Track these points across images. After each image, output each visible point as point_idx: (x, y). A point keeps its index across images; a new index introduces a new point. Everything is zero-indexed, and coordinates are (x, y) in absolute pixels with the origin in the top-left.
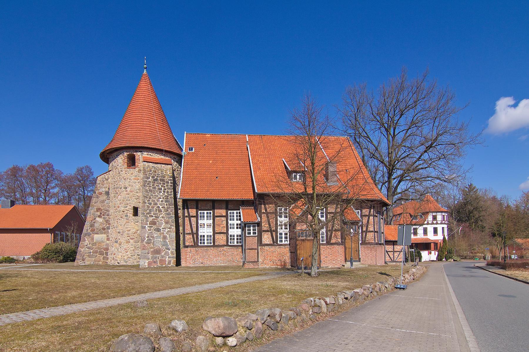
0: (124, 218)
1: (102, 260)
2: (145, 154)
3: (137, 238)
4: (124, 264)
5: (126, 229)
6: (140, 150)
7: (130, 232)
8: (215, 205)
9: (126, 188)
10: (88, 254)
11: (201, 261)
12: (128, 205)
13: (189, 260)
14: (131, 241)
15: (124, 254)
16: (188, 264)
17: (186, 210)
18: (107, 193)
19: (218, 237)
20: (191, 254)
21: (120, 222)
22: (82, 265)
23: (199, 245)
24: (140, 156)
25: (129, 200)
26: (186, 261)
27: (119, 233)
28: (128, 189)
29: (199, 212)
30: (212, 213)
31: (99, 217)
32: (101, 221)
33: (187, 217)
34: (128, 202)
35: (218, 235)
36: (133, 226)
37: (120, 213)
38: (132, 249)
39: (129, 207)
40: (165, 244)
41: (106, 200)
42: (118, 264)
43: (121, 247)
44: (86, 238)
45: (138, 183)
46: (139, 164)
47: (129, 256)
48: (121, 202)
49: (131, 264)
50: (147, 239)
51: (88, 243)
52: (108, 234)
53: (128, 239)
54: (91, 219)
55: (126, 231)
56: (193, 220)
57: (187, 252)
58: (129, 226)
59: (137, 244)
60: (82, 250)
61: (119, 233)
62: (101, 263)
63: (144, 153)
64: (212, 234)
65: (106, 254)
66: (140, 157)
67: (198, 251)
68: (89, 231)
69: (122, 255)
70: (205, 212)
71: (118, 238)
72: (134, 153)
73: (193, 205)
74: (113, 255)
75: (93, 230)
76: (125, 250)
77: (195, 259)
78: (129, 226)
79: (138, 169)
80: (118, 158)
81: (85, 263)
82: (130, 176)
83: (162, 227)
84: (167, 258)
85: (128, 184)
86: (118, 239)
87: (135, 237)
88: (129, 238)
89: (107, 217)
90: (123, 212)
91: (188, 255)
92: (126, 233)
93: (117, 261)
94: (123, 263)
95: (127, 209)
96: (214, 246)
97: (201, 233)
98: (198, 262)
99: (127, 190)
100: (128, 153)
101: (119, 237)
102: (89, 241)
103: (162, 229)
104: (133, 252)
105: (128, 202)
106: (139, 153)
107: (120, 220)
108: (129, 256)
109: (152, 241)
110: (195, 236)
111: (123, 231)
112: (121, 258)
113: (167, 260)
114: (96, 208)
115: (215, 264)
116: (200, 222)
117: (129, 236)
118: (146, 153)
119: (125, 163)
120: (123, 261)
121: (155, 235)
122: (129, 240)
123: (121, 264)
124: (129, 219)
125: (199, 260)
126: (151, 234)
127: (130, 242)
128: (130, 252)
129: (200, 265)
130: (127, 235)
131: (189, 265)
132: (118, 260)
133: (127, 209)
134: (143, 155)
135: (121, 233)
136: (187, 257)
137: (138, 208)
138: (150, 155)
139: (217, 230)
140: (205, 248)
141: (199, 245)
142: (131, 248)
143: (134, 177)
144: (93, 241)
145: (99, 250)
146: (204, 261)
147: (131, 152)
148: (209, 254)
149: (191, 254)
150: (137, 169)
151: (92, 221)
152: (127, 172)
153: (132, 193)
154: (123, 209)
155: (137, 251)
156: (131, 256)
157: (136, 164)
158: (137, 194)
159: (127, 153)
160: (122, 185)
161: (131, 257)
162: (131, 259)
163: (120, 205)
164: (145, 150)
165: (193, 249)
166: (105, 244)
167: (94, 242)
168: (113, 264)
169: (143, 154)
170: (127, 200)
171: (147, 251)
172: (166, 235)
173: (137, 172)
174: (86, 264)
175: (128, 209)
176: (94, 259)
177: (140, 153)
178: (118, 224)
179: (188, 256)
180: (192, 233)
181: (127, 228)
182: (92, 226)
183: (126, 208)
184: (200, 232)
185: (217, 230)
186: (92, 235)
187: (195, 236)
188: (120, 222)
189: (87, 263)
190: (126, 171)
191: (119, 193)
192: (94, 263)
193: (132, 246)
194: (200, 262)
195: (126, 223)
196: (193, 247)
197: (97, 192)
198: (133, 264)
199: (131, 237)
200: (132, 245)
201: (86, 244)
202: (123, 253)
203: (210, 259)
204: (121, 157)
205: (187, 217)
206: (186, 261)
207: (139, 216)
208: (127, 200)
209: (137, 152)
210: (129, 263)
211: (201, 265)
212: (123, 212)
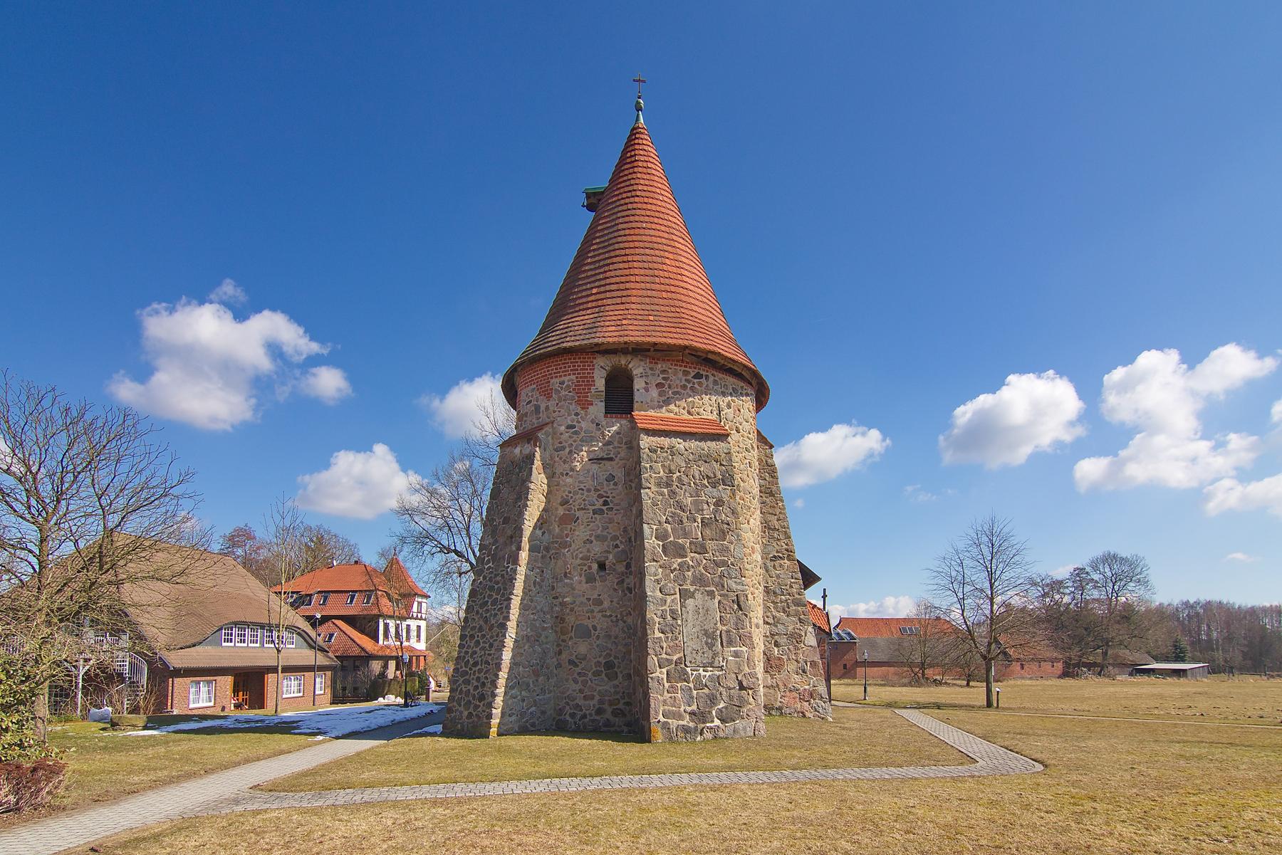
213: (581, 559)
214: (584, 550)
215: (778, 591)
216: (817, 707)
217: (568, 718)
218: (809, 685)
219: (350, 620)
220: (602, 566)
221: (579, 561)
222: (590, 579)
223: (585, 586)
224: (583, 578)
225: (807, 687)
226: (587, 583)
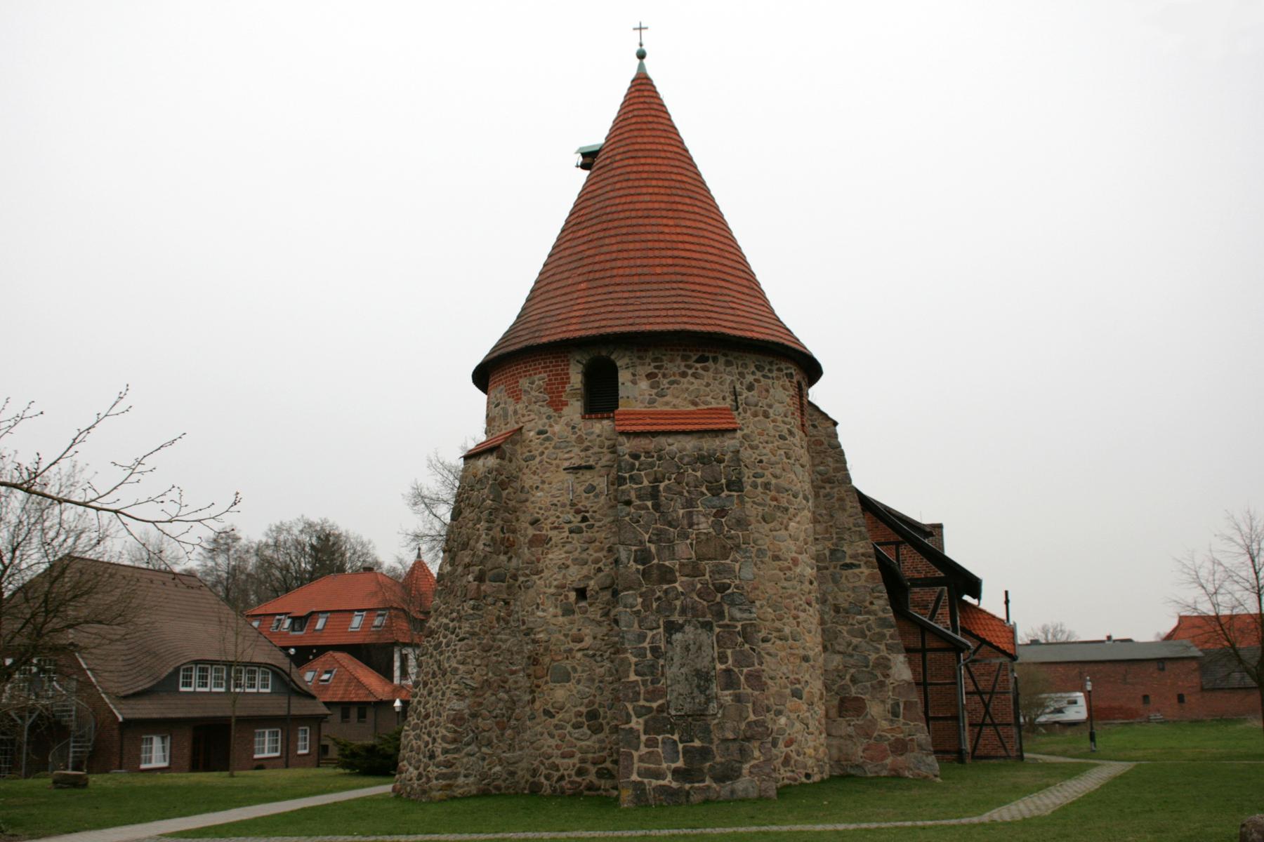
74: (781, 744)
213: (557, 587)
214: (560, 576)
217: (543, 779)
219: (358, 651)
220: (582, 593)
221: (553, 590)
222: (568, 611)
223: (561, 619)
224: (559, 611)
226: (563, 615)
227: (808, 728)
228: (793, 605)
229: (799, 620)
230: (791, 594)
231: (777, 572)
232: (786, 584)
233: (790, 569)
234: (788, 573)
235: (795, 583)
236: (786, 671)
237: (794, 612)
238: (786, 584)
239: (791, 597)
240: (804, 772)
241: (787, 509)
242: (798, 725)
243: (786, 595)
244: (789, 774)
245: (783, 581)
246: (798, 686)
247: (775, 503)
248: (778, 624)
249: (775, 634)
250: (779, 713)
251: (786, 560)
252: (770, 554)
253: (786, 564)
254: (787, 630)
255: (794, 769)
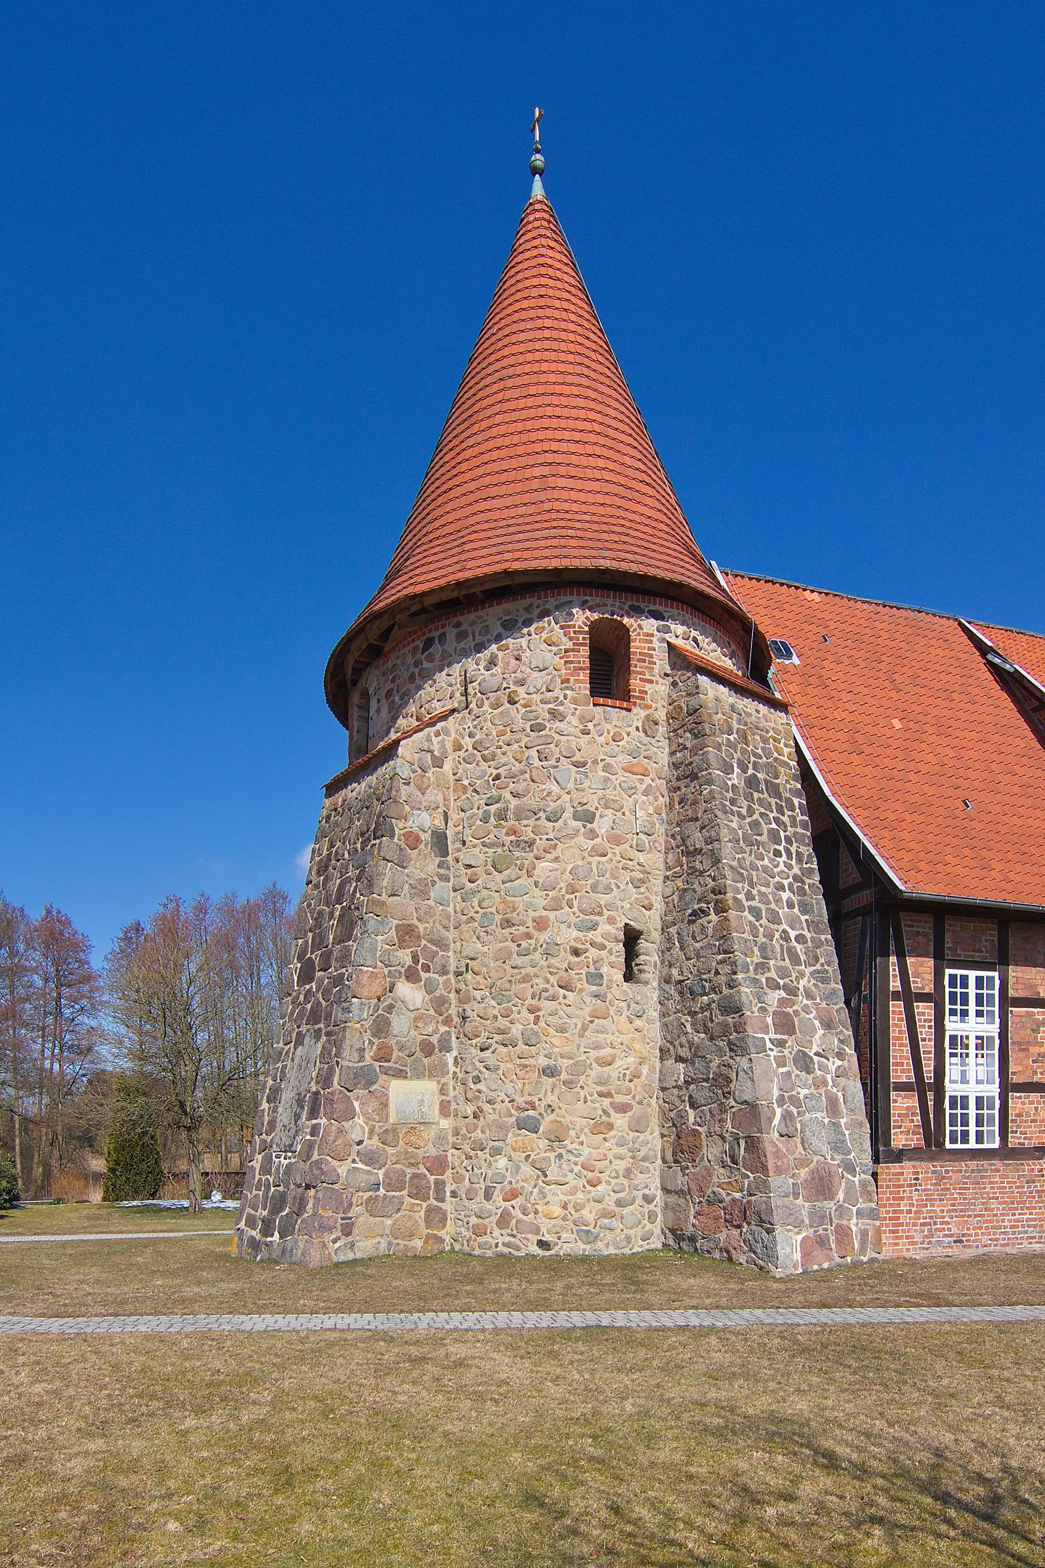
0: (581, 990)
1: (423, 1225)
2: (679, 633)
3: (640, 1103)
4: (582, 1248)
5: (594, 1054)
6: (652, 607)
7: (613, 1072)
8: (1010, 942)
9: (588, 817)
10: (366, 1195)
11: (955, 1230)
12: (600, 914)
13: (908, 1224)
14: (620, 1121)
15: (580, 1195)
16: (904, 1244)
17: (893, 959)
18: (440, 841)
19: (1020, 1105)
20: (915, 1196)
21: (553, 1014)
22: (342, 1258)
23: (948, 1145)
24: (655, 639)
25: (608, 890)
26: (894, 1232)
27: (550, 1072)
28: (602, 825)
29: (948, 972)
30: (997, 982)
31: (407, 977)
32: (419, 1003)
33: (896, 996)
34: (603, 899)
35: (1018, 1095)
36: (625, 1038)
37: (553, 961)
38: (621, 1165)
39: (604, 928)
40: (838, 1147)
41: (437, 879)
42: (540, 1252)
43: (560, 1156)
44: (357, 1099)
45: (646, 793)
46: (648, 687)
47: (610, 1203)
48: (554, 899)
49: (618, 1252)
50: (779, 1112)
51: (367, 1129)
52: (443, 1081)
53: (604, 1111)
54: (376, 988)
55: (594, 1064)
56: (924, 1011)
57: (902, 1186)
58: (609, 1038)
59: (642, 1136)
60: (340, 1171)
61: (550, 1072)
62: (418, 1243)
63: (672, 627)
64: (993, 1090)
65: (437, 1191)
66: (656, 644)
67: (943, 1178)
68: (368, 1060)
69: (565, 1198)
70: (972, 975)
71: (543, 1104)
72: (626, 620)
73: (925, 935)
74: (497, 1196)
75: (383, 1056)
76: (585, 1172)
77: (931, 1218)
78: (609, 1038)
79: (643, 714)
80: (524, 642)
81: (353, 1245)
82: (607, 749)
83: (815, 1049)
84: (854, 1221)
85: (600, 793)
86: (542, 1109)
87: (634, 1097)
88: (606, 1101)
89: (442, 979)
90: (576, 952)
91: (902, 1199)
92: (593, 1073)
93: (537, 1231)
94: (570, 1245)
95: (596, 936)
96: (1005, 1152)
97: (954, 1086)
98: (945, 1236)
99: (592, 831)
100: (596, 616)
101: (551, 1099)
102: (368, 1119)
103: (816, 1059)
104: (626, 1182)
105: (603, 899)
106: (650, 625)
107: (554, 998)
108: (610, 1203)
109: (799, 1126)
110: (930, 1096)
111: (575, 1064)
112: (564, 1219)
113: (854, 1228)
114: (395, 922)
115: (1007, 1245)
116: (952, 1026)
117: (608, 1095)
118: (680, 629)
119: (581, 669)
120: (575, 1236)
121: (804, 1092)
122: (609, 1116)
123: (561, 1249)
124: (609, 996)
125: (947, 1223)
126: (789, 1084)
127: (610, 1127)
128: (613, 1182)
129: (950, 1251)
130: (599, 1088)
131: (908, 1250)
132: (544, 1230)
133: (596, 936)
134: (667, 636)
135: (564, 1076)
136: (902, 1211)
137: (641, 933)
138: (695, 640)
139: (1018, 1073)
140: (973, 1164)
141: (948, 1145)
142: (618, 1162)
143: (623, 759)
144: (387, 1121)
145: (409, 1171)
146: (969, 1229)
147: (609, 608)
148: (988, 1193)
149: (915, 1196)
150: (639, 714)
151: (379, 1000)
152: (590, 726)
153: (617, 850)
154: (576, 940)
155: (640, 1179)
156: (619, 1203)
157: (635, 682)
158: (641, 857)
159: (588, 613)
160: (567, 797)
161: (617, 1209)
162: (615, 1223)
163: (552, 915)
164: (677, 608)
165: (925, 1168)
166: (432, 1133)
167: (391, 1120)
168: (501, 1248)
169: (668, 630)
170: (594, 888)
171: (791, 1181)
172: (835, 1090)
173: (637, 729)
174: (359, 1255)
175: (599, 940)
176: (389, 1222)
177: (652, 621)
178: (542, 1024)
179: (903, 1206)
180: (919, 1086)
181: (598, 1047)
182: (381, 1027)
183: (591, 935)
184: (951, 1082)
185: (1018, 1073)
186: (380, 1082)
187: (930, 1096)
188: (553, 1014)
189: (365, 1247)
190: (583, 719)
191: (540, 843)
192: (390, 1244)
193: (623, 1151)
194: (952, 1236)
195: (595, 1015)
196: (921, 1160)
197: (399, 826)
198: (627, 1251)
199: (619, 1099)
200: (621, 1144)
201: (356, 1136)
202: (573, 1193)
203: (991, 1221)
204: (544, 635)
205: (896, 996)
206: (894, 1232)
207: (646, 983)
208: (594, 888)
209: (636, 611)
210: (607, 1245)
211: (958, 1252)
212: (576, 952)
215: (697, 989)
216: (753, 1242)
218: (742, 1191)
225: (737, 1195)
227: (546, 1176)
228: (530, 991)
229: (541, 1013)
230: (527, 975)
231: (510, 944)
232: (519, 961)
233: (528, 936)
234: (524, 944)
235: (537, 956)
236: (510, 1091)
237: (529, 1001)
238: (519, 961)
239: (527, 979)
240: (534, 1239)
241: (531, 844)
242: (527, 1170)
243: (518, 977)
244: (508, 1239)
245: (515, 955)
246: (531, 1113)
247: (513, 838)
248: (502, 1023)
249: (497, 1037)
250: (496, 1152)
251: (523, 923)
252: (498, 918)
253: (523, 929)
254: (516, 1030)
255: (515, 1232)
